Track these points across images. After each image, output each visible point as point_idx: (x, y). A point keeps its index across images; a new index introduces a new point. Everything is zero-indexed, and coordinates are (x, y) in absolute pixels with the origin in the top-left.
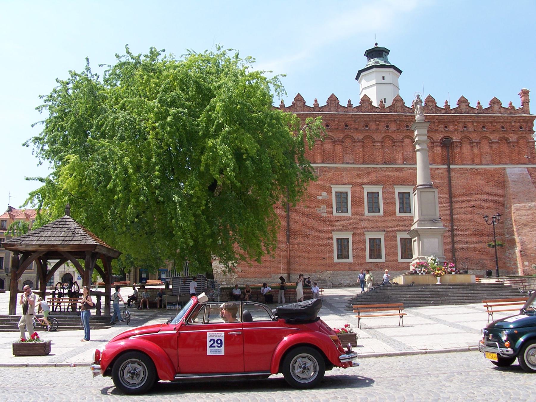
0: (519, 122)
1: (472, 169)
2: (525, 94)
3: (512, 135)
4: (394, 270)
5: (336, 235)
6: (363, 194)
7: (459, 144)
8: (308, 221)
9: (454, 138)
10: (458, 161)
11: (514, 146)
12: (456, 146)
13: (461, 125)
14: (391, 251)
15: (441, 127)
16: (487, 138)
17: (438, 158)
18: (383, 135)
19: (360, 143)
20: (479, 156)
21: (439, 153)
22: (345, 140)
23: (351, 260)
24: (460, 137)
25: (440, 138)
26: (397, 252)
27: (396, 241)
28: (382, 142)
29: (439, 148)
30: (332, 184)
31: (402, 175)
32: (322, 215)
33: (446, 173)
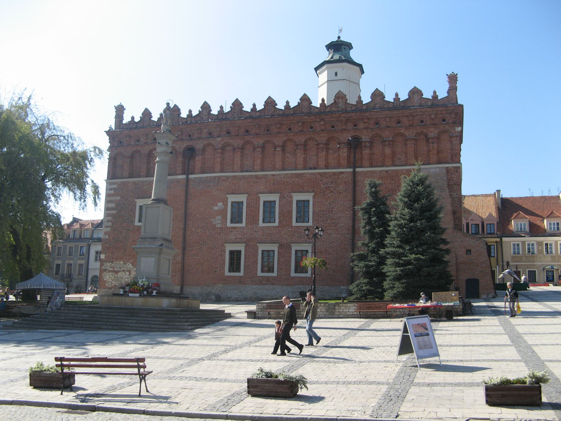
1: (381, 172)
2: (453, 79)
3: (432, 129)
5: (230, 247)
7: (368, 144)
8: (204, 232)
9: (363, 137)
10: (366, 163)
11: (433, 143)
12: (365, 146)
13: (372, 122)
15: (350, 126)
16: (402, 135)
18: (285, 139)
21: (345, 155)
24: (370, 135)
26: (290, 266)
27: (291, 253)
30: (228, 194)
32: (217, 226)
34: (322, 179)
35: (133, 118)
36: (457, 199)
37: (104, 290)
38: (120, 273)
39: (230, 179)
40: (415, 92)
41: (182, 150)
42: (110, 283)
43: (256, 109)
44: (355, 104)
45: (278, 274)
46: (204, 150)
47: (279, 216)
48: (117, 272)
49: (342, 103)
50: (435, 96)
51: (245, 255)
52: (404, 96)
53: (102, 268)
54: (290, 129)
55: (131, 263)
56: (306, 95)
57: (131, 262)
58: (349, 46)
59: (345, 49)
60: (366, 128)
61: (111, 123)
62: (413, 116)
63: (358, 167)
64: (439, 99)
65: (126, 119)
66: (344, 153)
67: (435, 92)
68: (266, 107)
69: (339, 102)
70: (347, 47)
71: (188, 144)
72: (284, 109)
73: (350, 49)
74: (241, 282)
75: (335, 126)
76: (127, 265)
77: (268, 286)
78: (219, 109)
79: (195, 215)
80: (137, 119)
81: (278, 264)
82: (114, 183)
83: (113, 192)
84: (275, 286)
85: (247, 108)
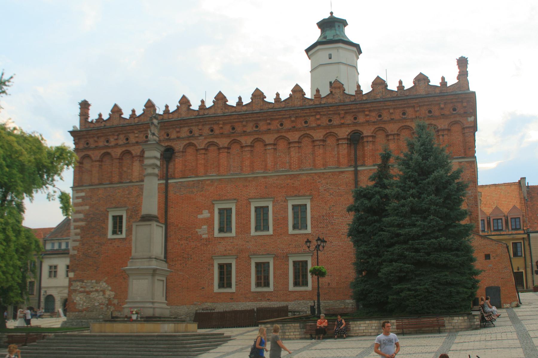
0: (452, 103)
2: (462, 63)
11: (443, 135)
15: (349, 119)
19: (249, 149)
21: (345, 152)
23: (233, 289)
25: (347, 133)
27: (288, 265)
28: (275, 144)
29: (345, 146)
34: (320, 180)
35: (100, 115)
36: (473, 197)
38: (92, 294)
39: (216, 184)
42: (81, 305)
43: (243, 103)
44: (355, 94)
45: (274, 289)
47: (273, 223)
48: (88, 293)
49: (339, 94)
50: (443, 82)
51: (236, 268)
52: (408, 84)
53: (71, 288)
54: (281, 125)
55: (105, 282)
57: (104, 280)
58: (344, 23)
59: (339, 26)
61: (76, 123)
64: (448, 86)
65: (93, 116)
67: (443, 78)
68: (254, 101)
69: (335, 93)
70: (341, 25)
72: (274, 102)
73: (345, 26)
74: (233, 299)
75: (332, 120)
76: (101, 284)
78: (200, 104)
79: (177, 225)
80: (105, 117)
81: (274, 277)
82: (82, 191)
83: (80, 200)
85: (232, 102)
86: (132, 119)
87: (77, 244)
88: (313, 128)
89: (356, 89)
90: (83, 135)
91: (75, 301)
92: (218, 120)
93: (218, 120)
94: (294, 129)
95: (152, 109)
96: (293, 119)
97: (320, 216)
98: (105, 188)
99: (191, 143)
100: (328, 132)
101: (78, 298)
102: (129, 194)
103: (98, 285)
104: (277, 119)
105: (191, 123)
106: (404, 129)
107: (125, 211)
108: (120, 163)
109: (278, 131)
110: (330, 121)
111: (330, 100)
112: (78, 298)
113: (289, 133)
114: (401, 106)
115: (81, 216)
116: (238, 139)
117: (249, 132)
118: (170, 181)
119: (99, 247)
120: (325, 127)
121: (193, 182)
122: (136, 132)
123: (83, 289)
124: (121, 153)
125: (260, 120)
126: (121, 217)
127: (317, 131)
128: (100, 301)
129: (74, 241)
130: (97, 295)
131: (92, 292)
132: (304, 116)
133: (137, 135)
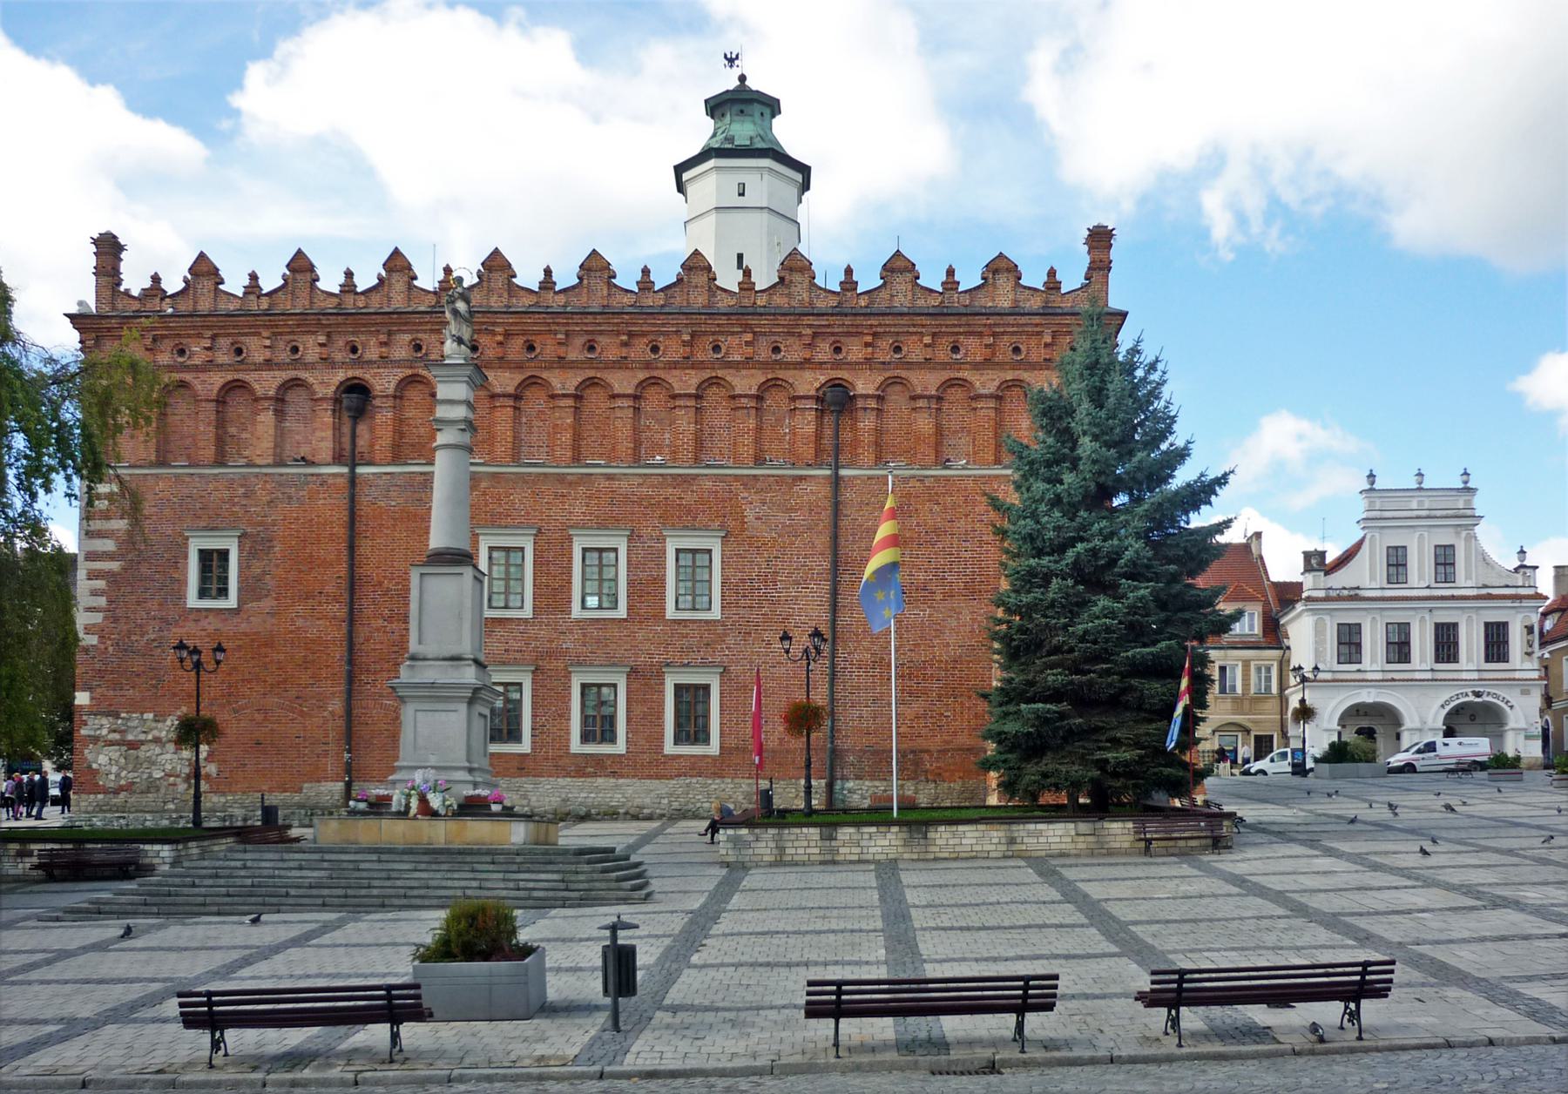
4: (650, 777)
6: (571, 553)
14: (646, 720)
16: (962, 383)
17: (805, 447)
19: (570, 402)
20: (933, 439)
21: (810, 429)
22: (528, 393)
25: (817, 385)
26: (661, 726)
28: (636, 397)
29: (811, 416)
31: (689, 498)
33: (826, 491)
34: (746, 495)
37: (92, 796)
38: (143, 748)
39: (484, 485)
40: (1001, 268)
41: (330, 391)
46: (399, 395)
54: (655, 349)
56: (700, 254)
60: (868, 361)
62: (994, 335)
63: (843, 467)
66: (806, 424)
68: (585, 282)
69: (791, 282)
71: (350, 374)
77: (600, 780)
79: (380, 584)
84: (621, 781)
85: (528, 277)
86: (252, 297)
87: (98, 618)
88: (736, 366)
89: (843, 279)
90: (109, 329)
91: (95, 766)
92: (494, 324)
93: (494, 324)
94: (688, 363)
95: (308, 276)
96: (686, 337)
97: (743, 581)
98: (177, 476)
99: (418, 375)
100: (769, 377)
101: (102, 759)
102: (246, 496)
103: (160, 725)
104: (643, 334)
105: (421, 324)
106: (953, 386)
107: (236, 540)
108: (218, 412)
109: (648, 366)
110: (776, 350)
111: (779, 300)
112: (102, 759)
113: (675, 372)
114: (948, 330)
115: (109, 545)
116: (545, 375)
117: (573, 362)
118: (360, 470)
119: (161, 630)
120: (765, 366)
121: (423, 478)
122: (265, 334)
123: (117, 736)
124: (224, 386)
125: (601, 333)
126: (224, 555)
127: (744, 372)
128: (168, 767)
129: (89, 609)
130: (158, 750)
131: (142, 743)
132: (714, 333)
133: (268, 342)
